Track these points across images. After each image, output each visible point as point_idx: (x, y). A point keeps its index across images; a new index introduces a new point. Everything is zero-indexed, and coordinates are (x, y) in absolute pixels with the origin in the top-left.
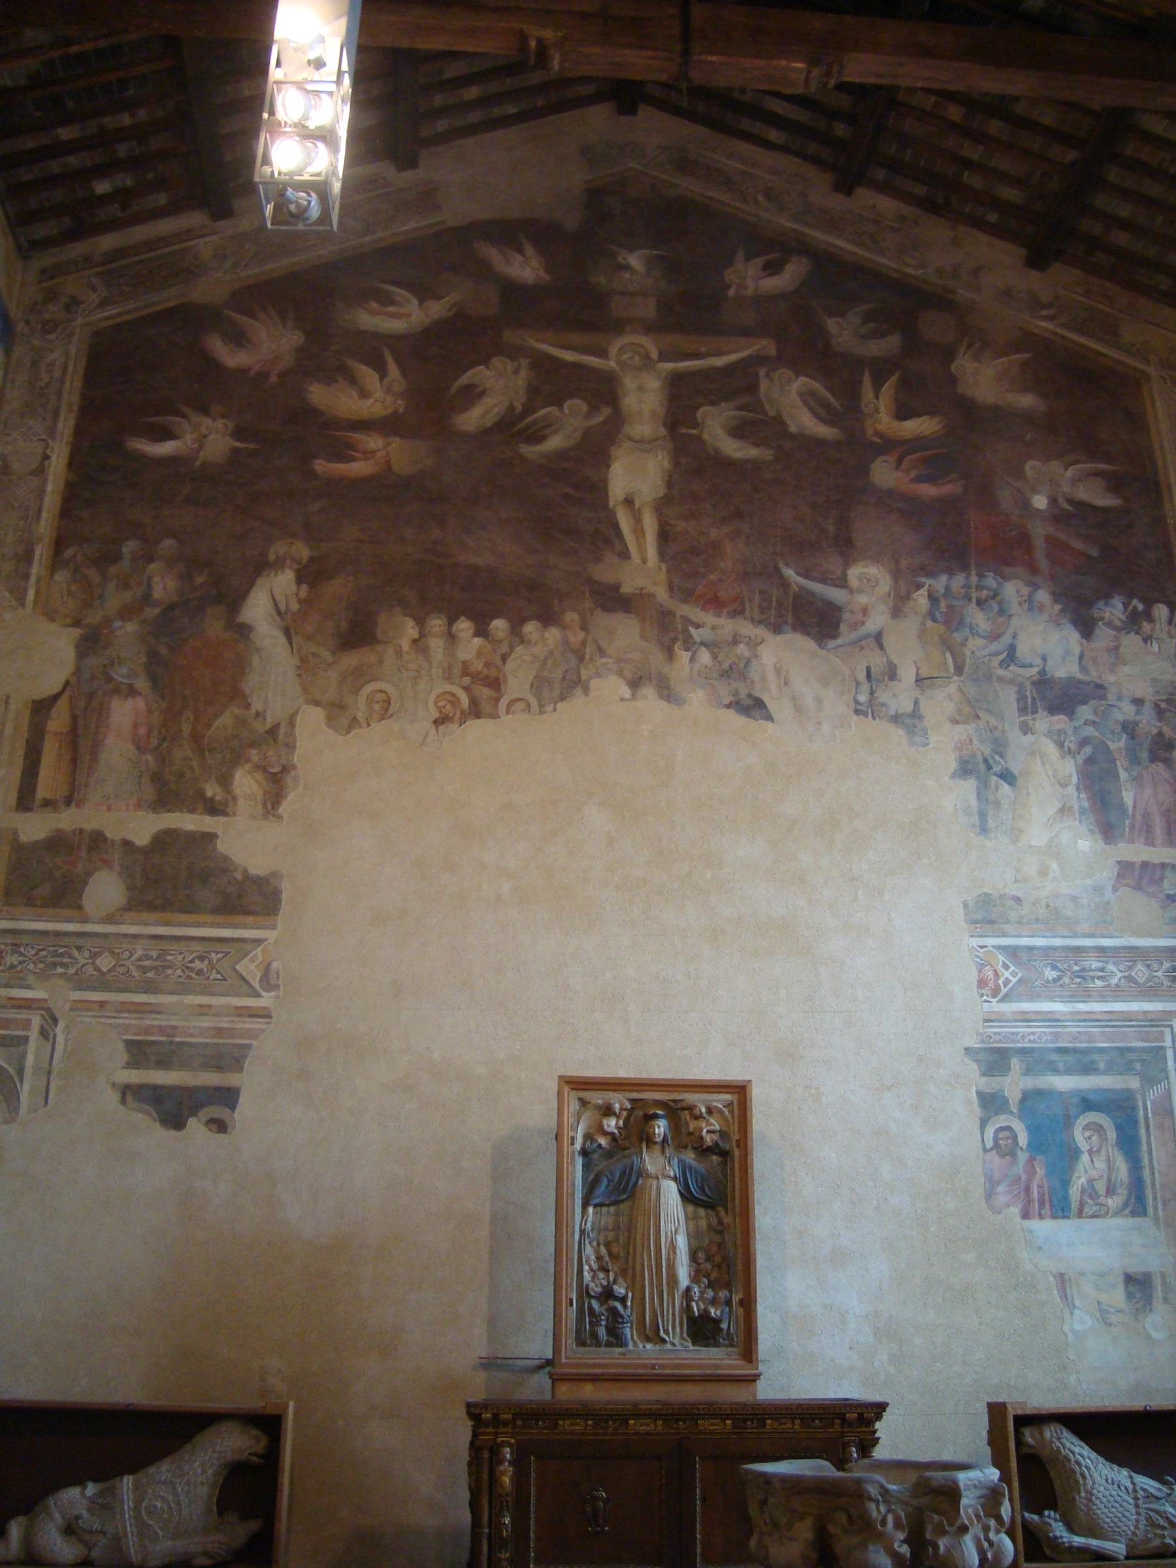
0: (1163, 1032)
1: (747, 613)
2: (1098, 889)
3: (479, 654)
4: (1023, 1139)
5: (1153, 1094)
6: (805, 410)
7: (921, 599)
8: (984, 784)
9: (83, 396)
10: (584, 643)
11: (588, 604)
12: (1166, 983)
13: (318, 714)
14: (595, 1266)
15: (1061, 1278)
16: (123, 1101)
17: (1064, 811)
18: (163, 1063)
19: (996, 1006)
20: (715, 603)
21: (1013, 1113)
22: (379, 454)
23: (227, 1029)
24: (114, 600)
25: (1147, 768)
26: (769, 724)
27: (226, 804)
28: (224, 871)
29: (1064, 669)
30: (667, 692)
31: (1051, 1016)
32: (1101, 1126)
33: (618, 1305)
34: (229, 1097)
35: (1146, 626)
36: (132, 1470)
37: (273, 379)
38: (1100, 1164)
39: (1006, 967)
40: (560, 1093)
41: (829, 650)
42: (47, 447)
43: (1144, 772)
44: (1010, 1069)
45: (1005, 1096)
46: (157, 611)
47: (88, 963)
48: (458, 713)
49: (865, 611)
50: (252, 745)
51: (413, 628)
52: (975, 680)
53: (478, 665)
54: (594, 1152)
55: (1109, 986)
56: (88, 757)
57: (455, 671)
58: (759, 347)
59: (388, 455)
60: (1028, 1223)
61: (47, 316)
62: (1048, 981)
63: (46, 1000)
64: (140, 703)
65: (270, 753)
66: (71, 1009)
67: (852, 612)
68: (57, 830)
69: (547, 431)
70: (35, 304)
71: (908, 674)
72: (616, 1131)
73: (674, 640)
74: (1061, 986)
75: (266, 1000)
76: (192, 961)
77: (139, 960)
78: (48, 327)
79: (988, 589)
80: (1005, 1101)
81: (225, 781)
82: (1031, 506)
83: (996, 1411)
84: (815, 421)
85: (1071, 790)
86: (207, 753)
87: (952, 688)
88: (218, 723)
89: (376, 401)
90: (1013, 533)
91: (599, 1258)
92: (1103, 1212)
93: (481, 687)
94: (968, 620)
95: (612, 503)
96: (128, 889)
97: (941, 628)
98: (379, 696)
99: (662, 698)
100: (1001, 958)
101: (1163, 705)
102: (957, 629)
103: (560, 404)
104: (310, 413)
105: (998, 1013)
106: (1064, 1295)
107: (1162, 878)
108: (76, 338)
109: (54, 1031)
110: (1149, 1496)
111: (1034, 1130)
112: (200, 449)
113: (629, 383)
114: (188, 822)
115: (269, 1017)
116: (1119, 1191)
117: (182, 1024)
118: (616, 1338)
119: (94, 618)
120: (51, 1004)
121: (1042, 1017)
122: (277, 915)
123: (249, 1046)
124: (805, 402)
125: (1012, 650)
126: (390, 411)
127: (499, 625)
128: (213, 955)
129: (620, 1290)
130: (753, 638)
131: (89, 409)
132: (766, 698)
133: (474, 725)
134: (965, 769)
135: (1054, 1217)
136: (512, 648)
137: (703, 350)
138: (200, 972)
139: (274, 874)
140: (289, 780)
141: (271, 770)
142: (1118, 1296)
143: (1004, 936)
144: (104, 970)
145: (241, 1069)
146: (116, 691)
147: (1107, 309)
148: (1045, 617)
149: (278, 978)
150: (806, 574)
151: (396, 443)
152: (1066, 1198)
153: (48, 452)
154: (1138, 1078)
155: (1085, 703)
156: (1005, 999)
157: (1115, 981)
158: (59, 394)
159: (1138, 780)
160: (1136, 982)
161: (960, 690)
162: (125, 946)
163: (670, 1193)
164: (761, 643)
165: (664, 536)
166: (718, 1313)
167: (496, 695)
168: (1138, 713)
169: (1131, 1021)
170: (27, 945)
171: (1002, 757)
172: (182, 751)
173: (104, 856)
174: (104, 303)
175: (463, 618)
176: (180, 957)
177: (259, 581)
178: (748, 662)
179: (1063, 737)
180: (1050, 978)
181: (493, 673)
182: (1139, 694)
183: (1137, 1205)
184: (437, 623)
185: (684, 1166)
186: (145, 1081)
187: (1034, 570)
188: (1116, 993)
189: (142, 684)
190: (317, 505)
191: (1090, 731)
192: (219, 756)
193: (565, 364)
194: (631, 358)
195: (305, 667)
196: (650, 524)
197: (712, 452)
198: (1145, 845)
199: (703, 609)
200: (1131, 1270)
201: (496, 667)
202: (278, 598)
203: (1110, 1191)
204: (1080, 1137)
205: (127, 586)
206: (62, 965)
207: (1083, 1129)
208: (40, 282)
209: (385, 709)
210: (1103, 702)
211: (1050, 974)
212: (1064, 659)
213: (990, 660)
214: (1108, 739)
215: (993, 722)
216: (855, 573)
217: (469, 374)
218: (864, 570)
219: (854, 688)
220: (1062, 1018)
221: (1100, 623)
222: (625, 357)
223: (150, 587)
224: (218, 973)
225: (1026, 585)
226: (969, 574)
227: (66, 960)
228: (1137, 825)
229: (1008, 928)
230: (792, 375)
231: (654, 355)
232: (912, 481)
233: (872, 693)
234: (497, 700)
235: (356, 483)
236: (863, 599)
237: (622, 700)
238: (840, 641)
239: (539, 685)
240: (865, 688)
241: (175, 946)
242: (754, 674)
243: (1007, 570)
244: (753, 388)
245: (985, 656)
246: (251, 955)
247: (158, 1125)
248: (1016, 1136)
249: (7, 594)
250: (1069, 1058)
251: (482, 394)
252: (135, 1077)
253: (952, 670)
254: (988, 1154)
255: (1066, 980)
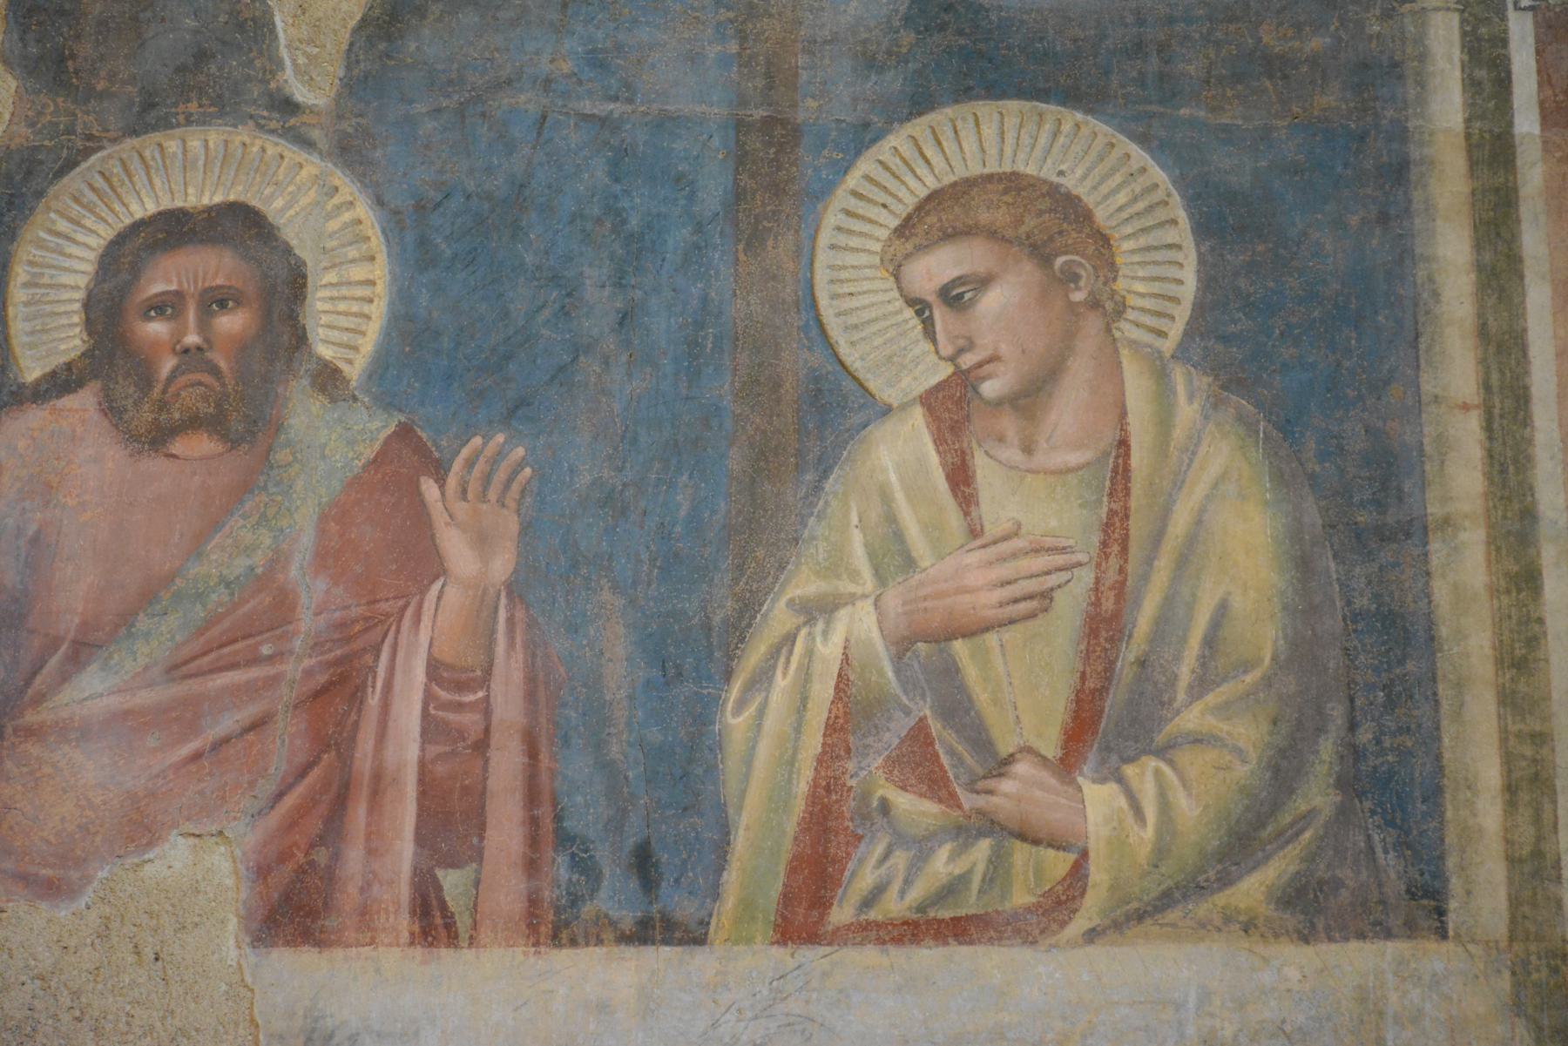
21: (288, 106)
32: (1070, 209)
92: (1021, 898)
116: (1192, 718)
207: (904, 230)
248: (297, 283)
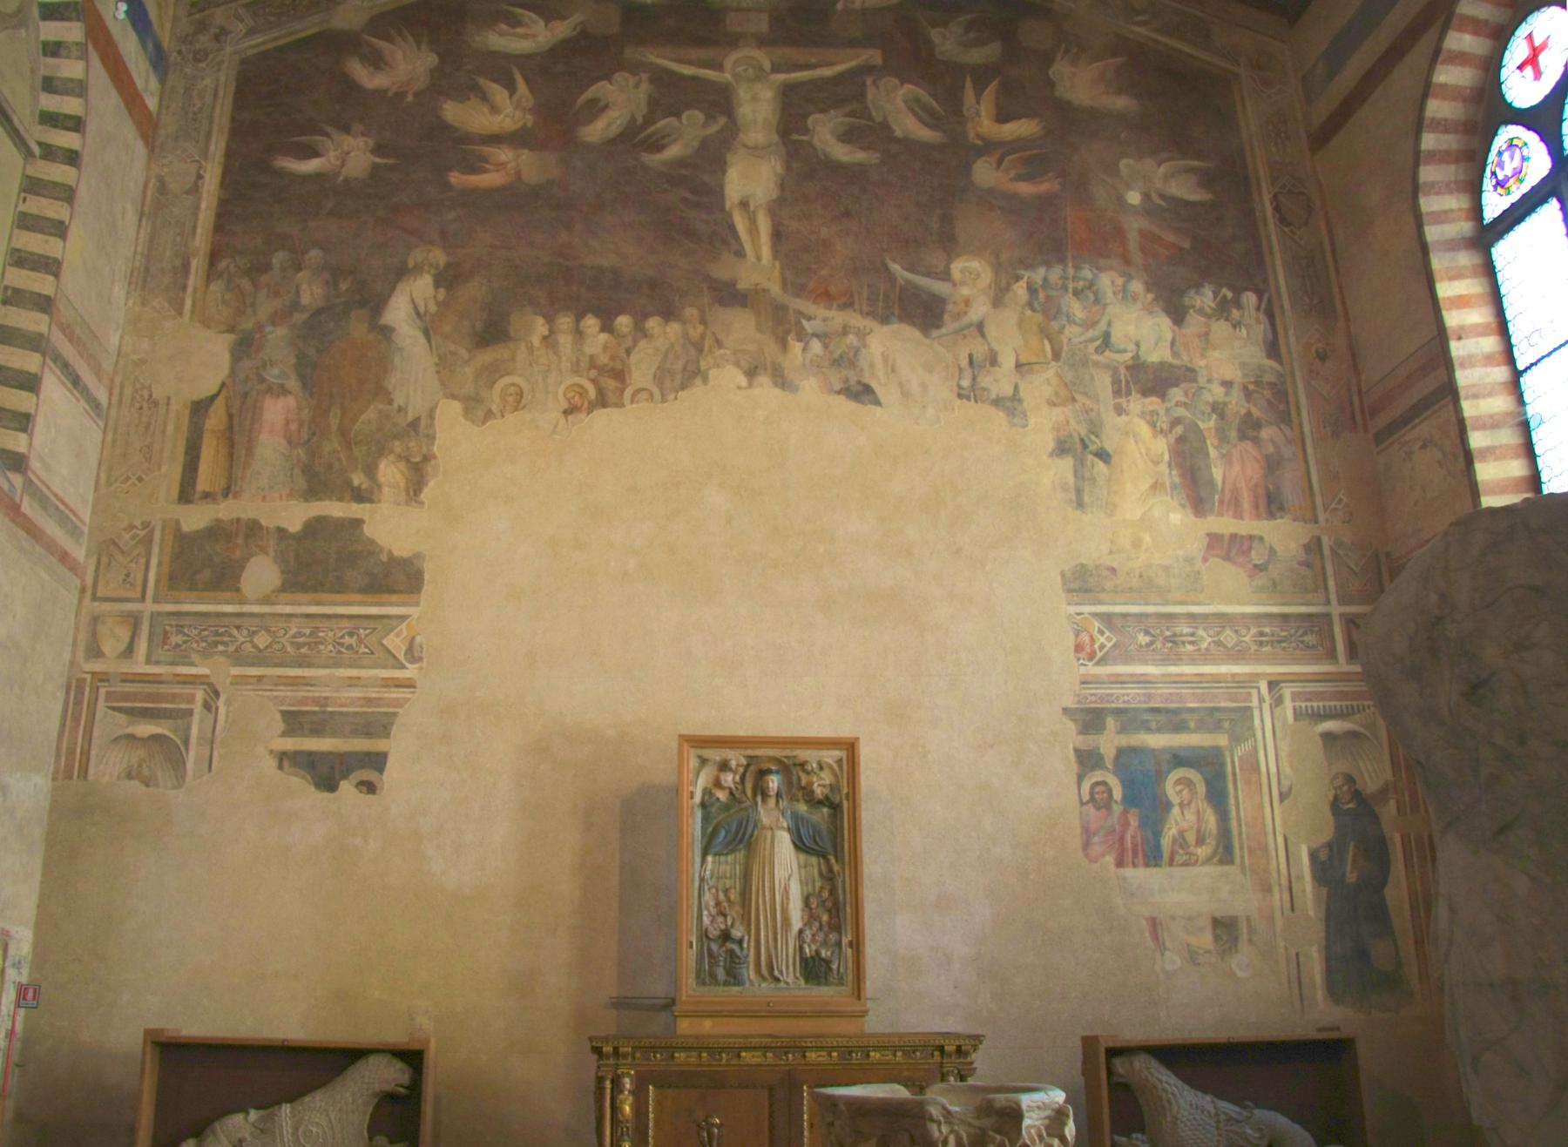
0: (1249, 694)
1: (856, 306)
2: (1189, 560)
3: (605, 348)
4: (1117, 793)
5: (1239, 751)
6: (911, 115)
7: (1020, 289)
8: (1080, 462)
9: (233, 119)
10: (703, 336)
11: (706, 300)
12: (1254, 647)
13: (456, 406)
14: (714, 911)
15: (1154, 923)
16: (280, 767)
17: (1156, 487)
18: (317, 731)
19: (1093, 669)
20: (826, 297)
21: (1107, 768)
22: (509, 166)
23: (375, 698)
24: (266, 306)
25: (1235, 446)
26: (878, 409)
27: (372, 492)
28: (371, 553)
29: (1156, 355)
30: (781, 380)
31: (1142, 679)
33: (735, 947)
34: (377, 761)
35: (1235, 313)
36: (291, 1099)
37: (410, 98)
38: (1190, 816)
39: (1101, 633)
40: (680, 752)
41: (934, 339)
42: (200, 167)
43: (1233, 451)
44: (1105, 728)
45: (1099, 754)
46: (305, 316)
47: (246, 642)
48: (586, 404)
49: (967, 302)
50: (396, 437)
51: (543, 325)
52: (1073, 365)
53: (604, 359)
54: (713, 804)
55: (1199, 650)
56: (244, 452)
57: (582, 365)
58: (864, 57)
59: (518, 165)
60: (1121, 871)
61: (198, 46)
62: (1141, 646)
63: (207, 676)
64: (291, 401)
65: (412, 444)
66: (232, 684)
67: (955, 303)
68: (217, 520)
69: (666, 141)
70: (187, 35)
71: (1008, 360)
72: (732, 786)
73: (788, 332)
74: (1154, 650)
75: (410, 672)
76: (342, 637)
77: (294, 637)
78: (199, 57)
79: (1085, 279)
80: (1101, 758)
81: (371, 472)
82: (1126, 201)
83: (1089, 1043)
84: (919, 125)
85: (1164, 468)
86: (353, 446)
87: (1050, 373)
88: (364, 417)
89: (506, 116)
90: (1108, 227)
91: (718, 904)
93: (606, 379)
94: (1065, 309)
95: (728, 205)
96: (283, 572)
97: (1039, 317)
98: (512, 389)
99: (776, 384)
100: (1097, 624)
101: (1251, 387)
102: (1055, 318)
103: (678, 115)
104: (446, 128)
105: (1093, 676)
106: (1155, 936)
107: (1250, 549)
108: (225, 65)
109: (215, 703)
110: (1230, 1119)
111: (1128, 784)
112: (343, 165)
113: (743, 93)
114: (337, 509)
115: (414, 687)
116: (1208, 841)
117: (335, 695)
118: (734, 977)
119: (248, 324)
120: (212, 680)
121: (1134, 679)
122: (419, 593)
123: (395, 714)
124: (912, 110)
125: (1106, 337)
126: (520, 125)
127: (623, 322)
128: (362, 631)
129: (737, 933)
130: (862, 328)
131: (238, 131)
132: (874, 385)
133: (601, 415)
134: (1062, 449)
135: (1147, 865)
136: (635, 342)
137: (813, 60)
138: (350, 647)
139: (418, 556)
140: (429, 468)
141: (413, 460)
142: (1206, 940)
143: (1100, 603)
144: (261, 646)
145: (387, 735)
146: (269, 390)
147: (1200, 14)
148: (1139, 305)
149: (421, 652)
150: (911, 268)
151: (525, 154)
152: (1157, 847)
153: (201, 172)
154: (1226, 735)
155: (1177, 385)
156: (1102, 662)
157: (1204, 645)
158: (211, 117)
159: (1227, 458)
160: (1225, 646)
161: (1057, 374)
162: (280, 625)
163: (784, 841)
164: (869, 334)
165: (778, 235)
166: (829, 953)
167: (619, 385)
168: (1227, 394)
169: (1220, 682)
170: (190, 626)
171: (1097, 436)
172: (331, 445)
173: (260, 543)
174: (252, 32)
175: (590, 315)
176: (331, 634)
177: (400, 287)
178: (857, 351)
179: (1155, 418)
180: (1143, 643)
181: (618, 366)
182: (1228, 377)
183: (1225, 853)
184: (565, 321)
185: (796, 817)
186: (299, 748)
187: (1126, 260)
188: (1205, 657)
189: (293, 383)
190: (452, 215)
191: (1181, 412)
192: (364, 448)
193: (682, 77)
194: (745, 70)
195: (444, 365)
196: (764, 225)
197: (823, 157)
198: (1235, 517)
199: (815, 302)
200: (1218, 915)
201: (622, 360)
202: (416, 301)
203: (1200, 841)
204: (1170, 789)
205: (277, 294)
206: (225, 644)
208: (190, 15)
209: (518, 401)
210: (1194, 385)
211: (1143, 639)
212: (1156, 344)
213: (1086, 347)
214: (1199, 419)
215: (1089, 403)
216: (957, 267)
217: (593, 88)
218: (967, 264)
219: (957, 374)
220: (1155, 680)
221: (1191, 311)
222: (740, 69)
223: (298, 292)
224: (366, 647)
225: (1121, 276)
226: (1066, 266)
227: (226, 639)
228: (1226, 500)
229: (1102, 596)
230: (897, 81)
231: (767, 66)
232: (1011, 180)
233: (974, 379)
234: (622, 391)
235: (489, 192)
236: (965, 291)
237: (739, 388)
238: (943, 331)
239: (661, 376)
240: (968, 374)
241: (327, 624)
242: (863, 362)
243: (1102, 262)
244: (860, 95)
245: (1081, 343)
246: (396, 631)
247: (312, 788)
249: (166, 305)
250: (1162, 718)
251: (606, 106)
252: (290, 744)
253: (1049, 355)
254: (1085, 807)
255: (1159, 645)
